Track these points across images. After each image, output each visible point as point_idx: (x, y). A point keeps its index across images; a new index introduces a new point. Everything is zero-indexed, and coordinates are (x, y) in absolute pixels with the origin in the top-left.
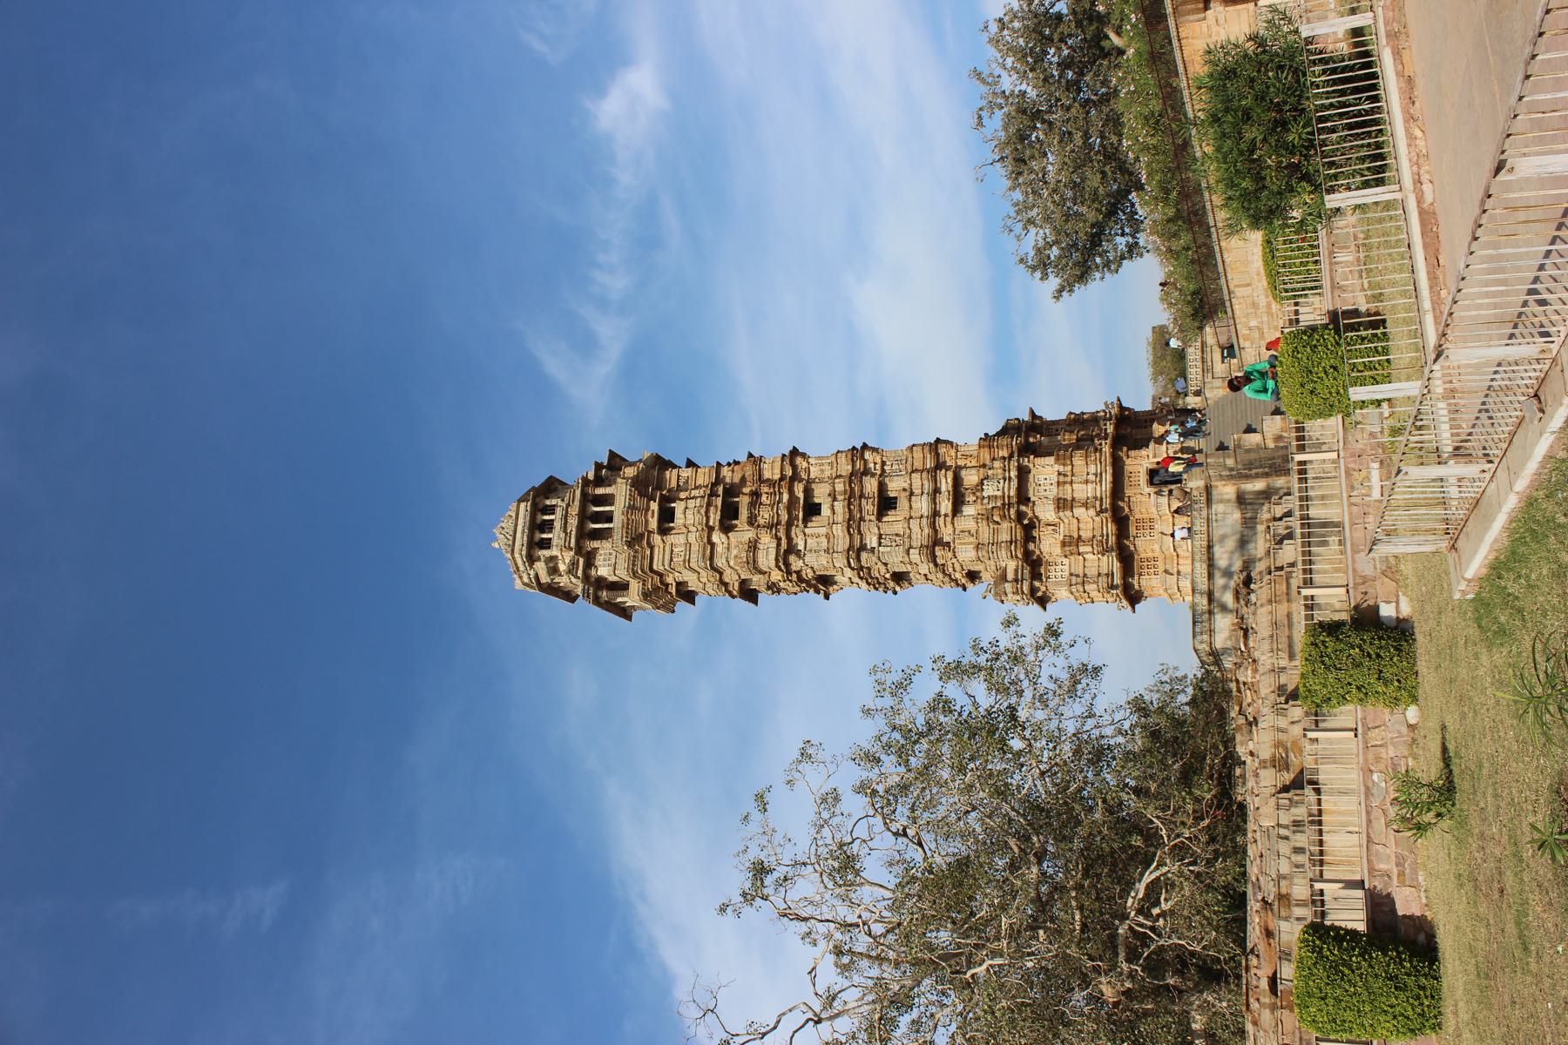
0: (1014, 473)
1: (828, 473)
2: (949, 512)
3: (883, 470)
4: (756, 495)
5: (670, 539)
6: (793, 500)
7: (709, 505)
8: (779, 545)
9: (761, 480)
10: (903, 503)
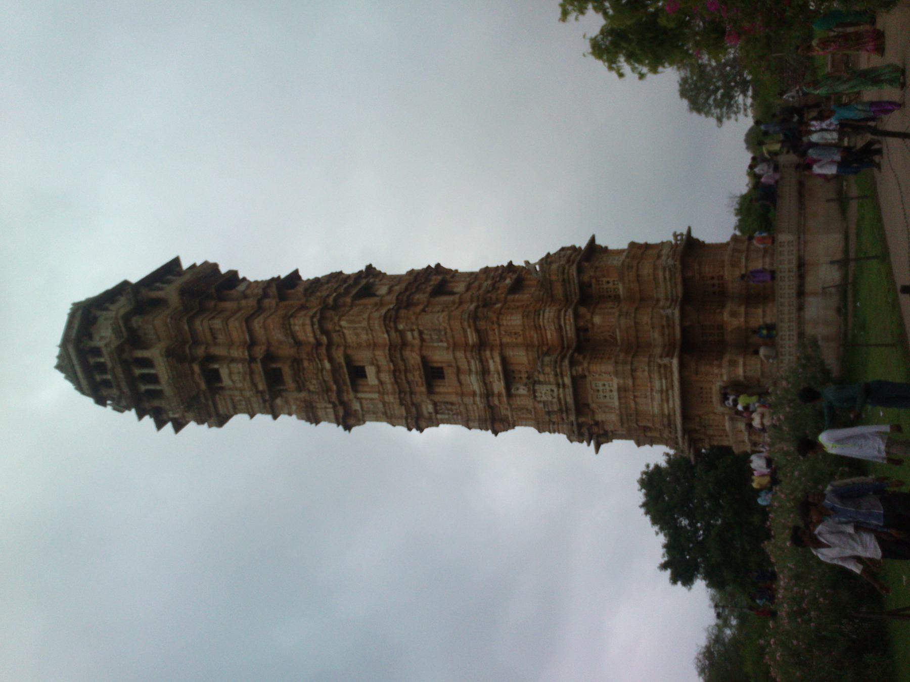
0: (567, 380)
1: (364, 337)
2: (504, 391)
3: (422, 340)
4: (296, 362)
5: (228, 392)
6: (335, 370)
7: (252, 372)
8: (335, 406)
9: (298, 343)
10: (450, 373)
